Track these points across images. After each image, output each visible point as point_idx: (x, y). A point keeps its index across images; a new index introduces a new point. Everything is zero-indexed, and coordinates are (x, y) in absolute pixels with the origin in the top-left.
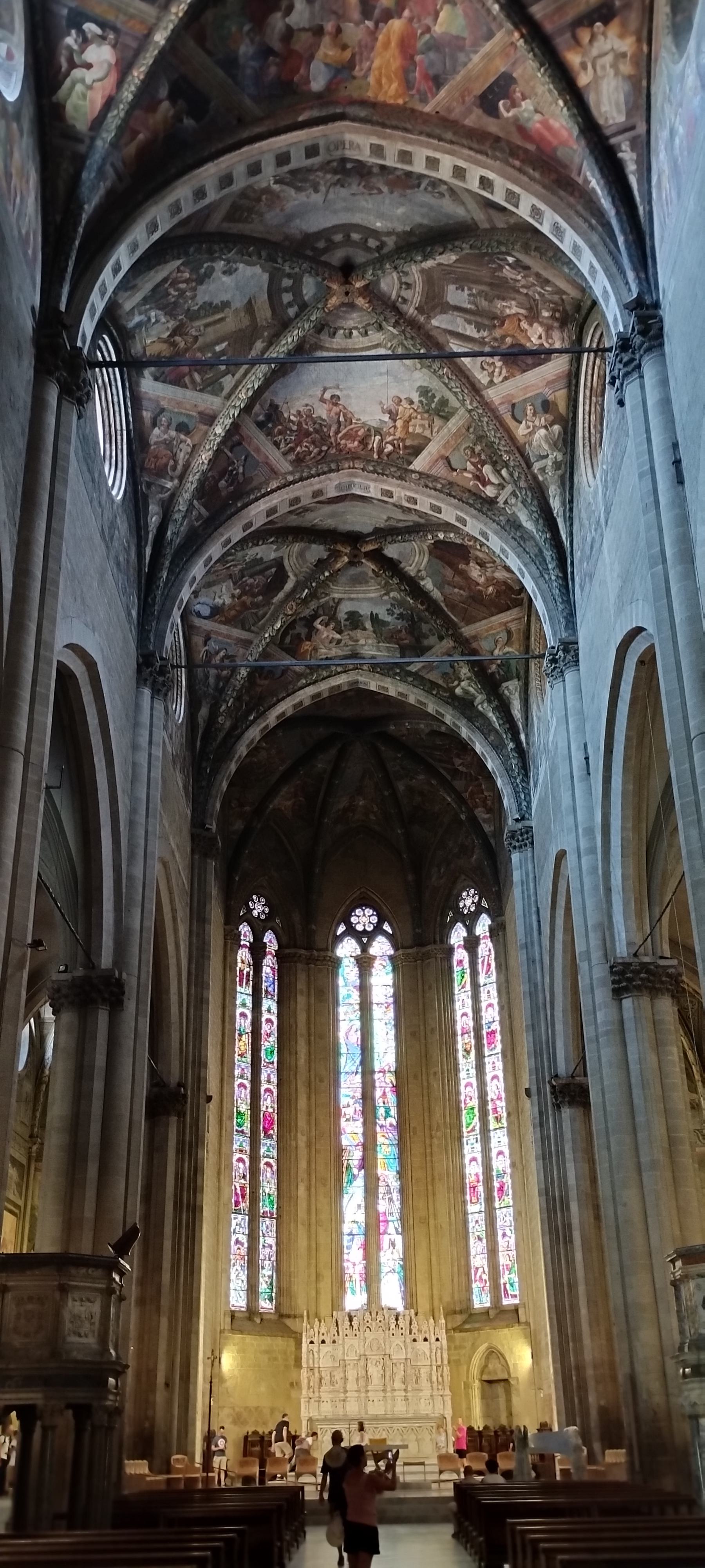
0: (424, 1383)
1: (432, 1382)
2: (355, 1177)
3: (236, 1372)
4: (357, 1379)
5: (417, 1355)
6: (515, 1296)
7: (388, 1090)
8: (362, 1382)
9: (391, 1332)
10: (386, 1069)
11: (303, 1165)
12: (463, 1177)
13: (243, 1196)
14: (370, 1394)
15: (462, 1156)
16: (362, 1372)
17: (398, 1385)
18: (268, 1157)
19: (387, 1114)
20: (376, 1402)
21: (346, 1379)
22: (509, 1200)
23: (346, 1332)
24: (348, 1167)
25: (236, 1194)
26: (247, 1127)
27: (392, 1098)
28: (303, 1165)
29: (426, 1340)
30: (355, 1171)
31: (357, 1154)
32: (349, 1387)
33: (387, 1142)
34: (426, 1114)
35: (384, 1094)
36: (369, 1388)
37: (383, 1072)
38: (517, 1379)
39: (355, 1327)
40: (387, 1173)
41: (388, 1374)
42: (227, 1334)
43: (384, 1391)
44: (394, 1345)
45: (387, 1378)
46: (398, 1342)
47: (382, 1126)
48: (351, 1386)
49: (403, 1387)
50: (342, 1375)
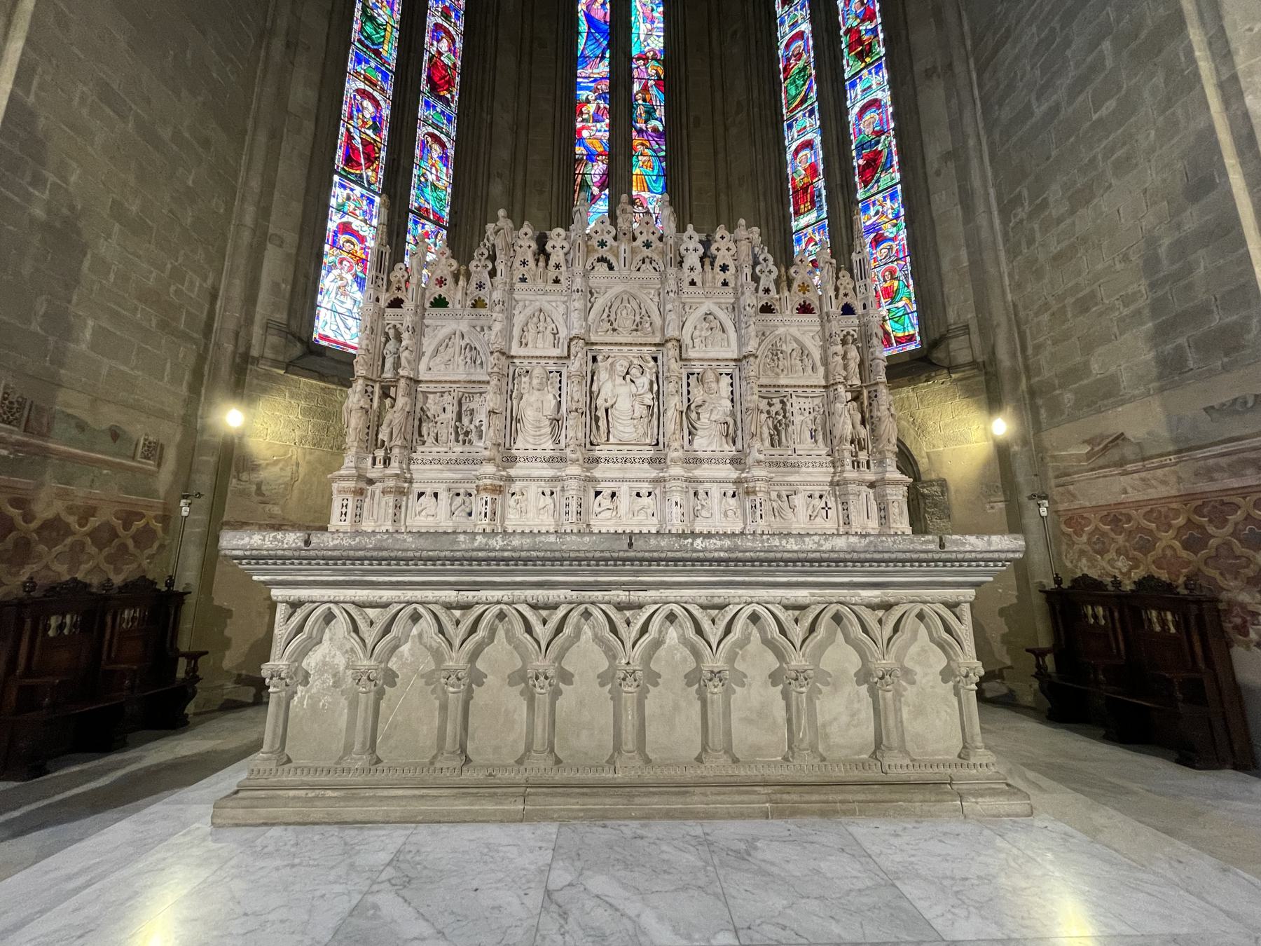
0: (802, 442)
1: (830, 437)
2: (594, 199)
3: (296, 453)
4: (556, 421)
5: (775, 353)
6: (911, 338)
7: (651, 83)
8: (573, 430)
9: (686, 275)
10: (650, 55)
11: (503, 154)
12: (782, 177)
13: (371, 160)
14: (598, 473)
15: (782, 150)
16: (575, 393)
17: (708, 441)
18: (437, 127)
19: (650, 113)
20: (624, 501)
21: (514, 421)
22: (891, 177)
23: (519, 271)
24: (584, 185)
25: (350, 148)
26: (390, 51)
27: (657, 97)
28: (503, 154)
29: (805, 309)
30: (596, 191)
31: (597, 169)
32: (522, 445)
33: (649, 152)
34: (718, 95)
35: (645, 89)
36: (601, 451)
37: (643, 57)
38: (943, 483)
39: (557, 257)
40: (646, 195)
41: (674, 404)
42: (263, 367)
43: (658, 461)
44: (694, 318)
45: (671, 415)
46: (708, 305)
47: (640, 131)
48: (533, 440)
49: (729, 450)
50: (492, 400)
